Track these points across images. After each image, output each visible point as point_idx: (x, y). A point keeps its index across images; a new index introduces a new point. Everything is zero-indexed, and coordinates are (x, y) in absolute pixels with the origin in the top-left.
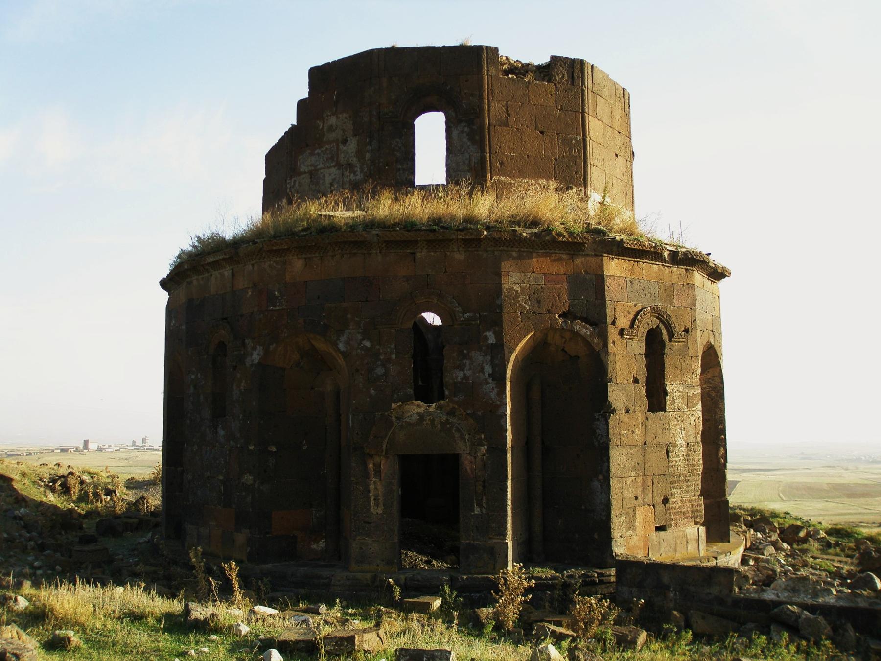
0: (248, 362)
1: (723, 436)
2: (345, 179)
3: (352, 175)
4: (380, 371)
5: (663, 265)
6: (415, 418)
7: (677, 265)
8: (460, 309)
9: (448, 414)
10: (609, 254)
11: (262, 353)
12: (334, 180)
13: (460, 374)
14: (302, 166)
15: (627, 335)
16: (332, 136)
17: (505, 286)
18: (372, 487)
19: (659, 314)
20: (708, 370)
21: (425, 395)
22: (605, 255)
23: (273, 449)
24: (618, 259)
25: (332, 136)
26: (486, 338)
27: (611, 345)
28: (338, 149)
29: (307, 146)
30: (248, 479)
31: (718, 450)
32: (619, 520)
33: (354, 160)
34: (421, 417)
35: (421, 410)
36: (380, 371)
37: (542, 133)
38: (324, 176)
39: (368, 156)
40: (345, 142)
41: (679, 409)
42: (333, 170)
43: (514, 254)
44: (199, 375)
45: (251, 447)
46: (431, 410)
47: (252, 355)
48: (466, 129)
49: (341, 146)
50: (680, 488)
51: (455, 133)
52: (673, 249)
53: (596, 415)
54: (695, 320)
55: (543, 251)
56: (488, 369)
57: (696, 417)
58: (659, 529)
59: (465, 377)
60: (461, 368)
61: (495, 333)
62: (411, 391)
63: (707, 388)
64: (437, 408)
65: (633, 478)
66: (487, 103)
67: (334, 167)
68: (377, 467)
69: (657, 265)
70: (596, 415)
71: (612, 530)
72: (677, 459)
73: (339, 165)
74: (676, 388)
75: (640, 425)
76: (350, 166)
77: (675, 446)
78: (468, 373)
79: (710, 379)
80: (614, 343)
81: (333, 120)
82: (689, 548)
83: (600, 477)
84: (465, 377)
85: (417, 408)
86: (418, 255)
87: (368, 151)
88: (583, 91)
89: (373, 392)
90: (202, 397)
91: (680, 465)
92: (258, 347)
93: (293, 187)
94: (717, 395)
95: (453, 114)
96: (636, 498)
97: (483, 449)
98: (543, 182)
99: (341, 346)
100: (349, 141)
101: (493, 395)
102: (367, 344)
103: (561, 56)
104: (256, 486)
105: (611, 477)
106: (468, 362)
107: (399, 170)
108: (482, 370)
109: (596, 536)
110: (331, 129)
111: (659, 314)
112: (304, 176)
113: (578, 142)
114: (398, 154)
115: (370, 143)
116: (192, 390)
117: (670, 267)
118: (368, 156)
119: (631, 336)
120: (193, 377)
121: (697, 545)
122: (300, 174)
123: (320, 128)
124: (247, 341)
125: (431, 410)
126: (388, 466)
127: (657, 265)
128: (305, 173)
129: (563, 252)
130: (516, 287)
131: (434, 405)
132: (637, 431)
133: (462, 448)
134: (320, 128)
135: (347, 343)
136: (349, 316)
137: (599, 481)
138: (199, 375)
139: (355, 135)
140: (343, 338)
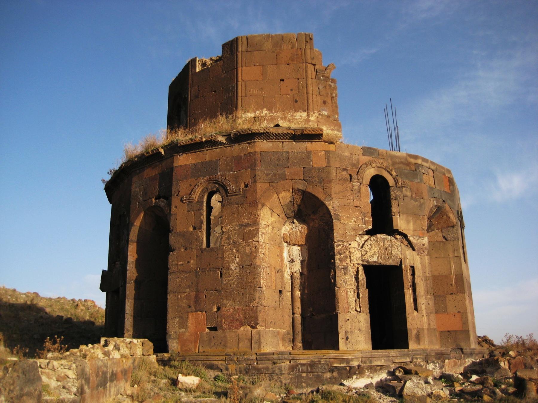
1: (332, 261)
5: (225, 147)
7: (238, 142)
10: (177, 153)
15: (186, 200)
17: (133, 190)
19: (215, 180)
20: (319, 210)
22: (174, 155)
24: (186, 154)
27: (173, 208)
31: (330, 272)
32: (174, 321)
41: (234, 243)
43: (138, 171)
50: (233, 300)
52: (302, 129)
54: (255, 176)
55: (149, 164)
57: (252, 247)
63: (322, 224)
65: (187, 293)
66: (190, 90)
69: (219, 148)
71: (167, 327)
72: (230, 278)
74: (231, 228)
75: (195, 257)
77: (228, 268)
79: (322, 217)
80: (176, 207)
82: (240, 345)
88: (237, 55)
91: (233, 283)
94: (328, 228)
96: (190, 307)
103: (226, 42)
105: (168, 292)
111: (215, 180)
113: (233, 87)
117: (233, 146)
119: (189, 200)
121: (249, 344)
127: (219, 148)
129: (157, 161)
132: (192, 261)
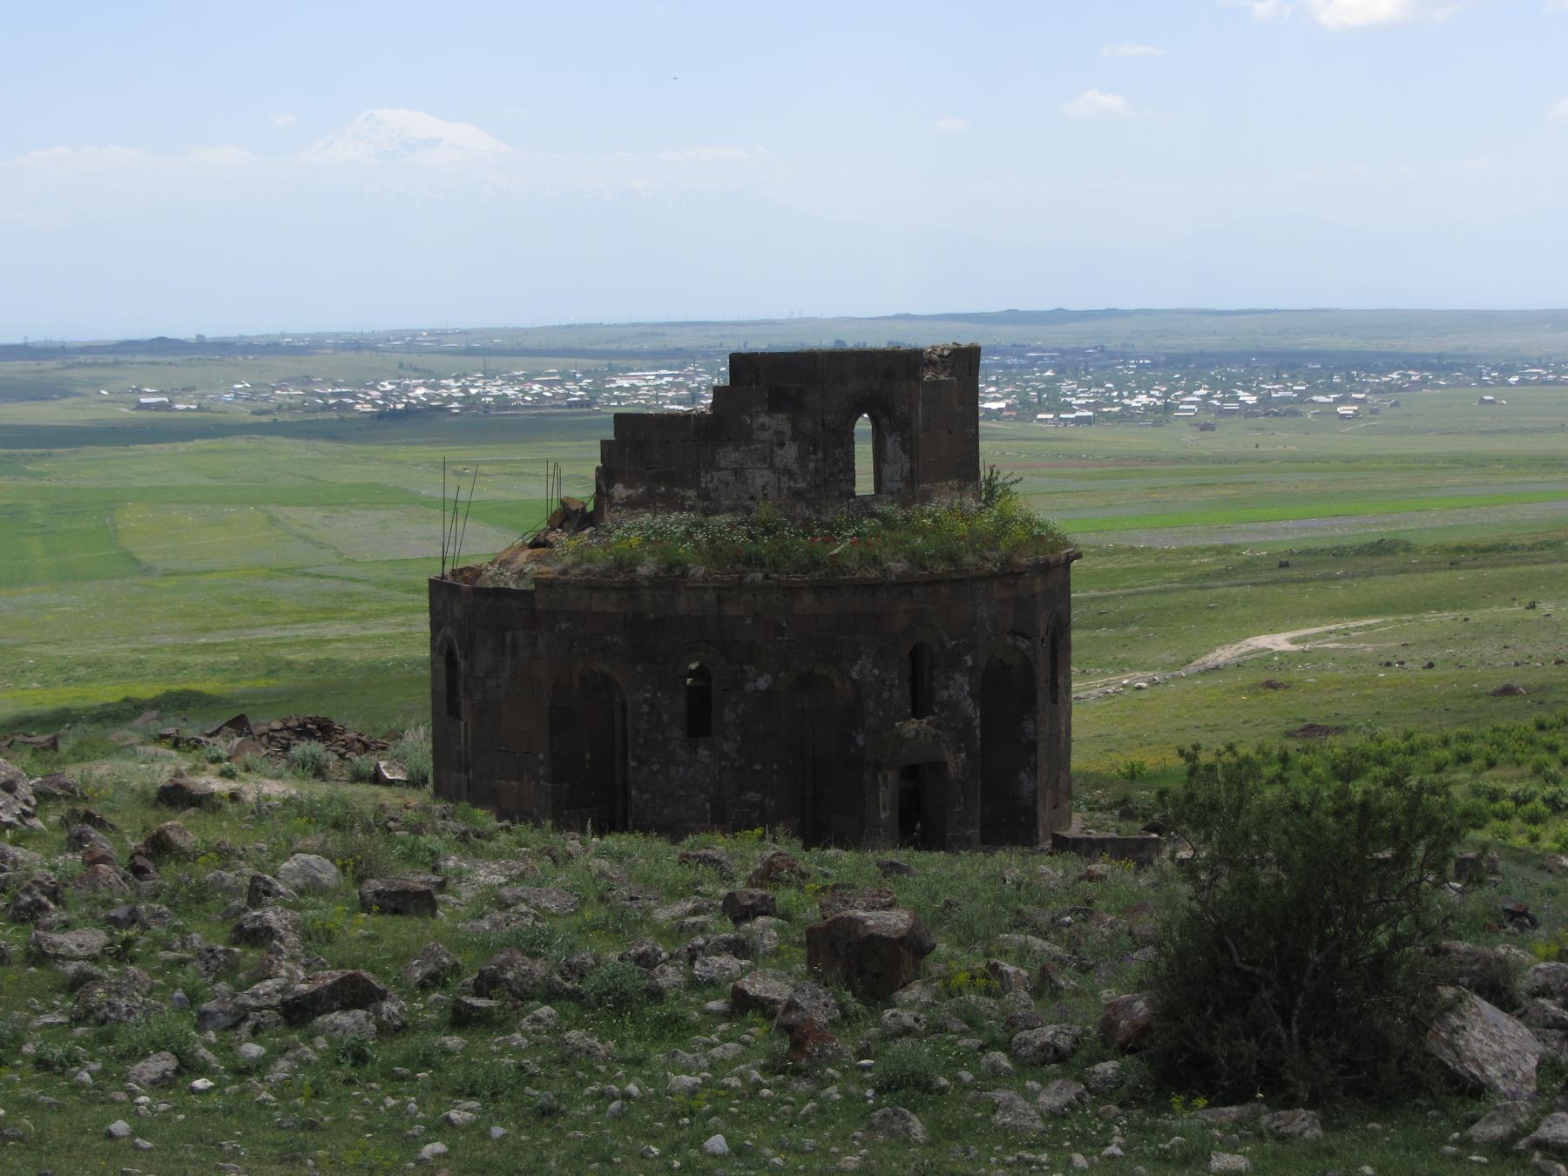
0: (749, 687)
2: (782, 485)
3: (792, 482)
4: (886, 695)
6: (913, 733)
8: (947, 638)
9: (935, 727)
11: (771, 680)
12: (767, 483)
13: (946, 694)
14: (722, 461)
16: (765, 435)
18: (881, 795)
21: (917, 713)
23: (775, 767)
25: (765, 435)
26: (966, 662)
28: (772, 450)
29: (729, 439)
30: (754, 796)
33: (795, 468)
34: (918, 733)
35: (915, 726)
36: (886, 695)
37: (950, 432)
38: (754, 477)
39: (812, 465)
40: (781, 445)
42: (767, 473)
44: (659, 694)
45: (758, 767)
46: (923, 725)
47: (755, 681)
48: (899, 438)
49: (776, 449)
51: (889, 443)
53: (1025, 716)
56: (967, 688)
58: (1055, 807)
59: (950, 696)
60: (947, 688)
61: (972, 656)
62: (909, 711)
64: (929, 723)
67: (768, 469)
68: (885, 778)
70: (1025, 716)
73: (772, 467)
76: (789, 473)
78: (952, 692)
81: (764, 419)
83: (1028, 769)
84: (950, 696)
85: (913, 726)
86: (915, 591)
87: (812, 460)
89: (881, 714)
90: (666, 717)
92: (765, 674)
93: (711, 482)
95: (888, 422)
97: (963, 755)
98: (950, 483)
99: (854, 675)
100: (787, 446)
101: (970, 709)
102: (876, 672)
104: (767, 802)
106: (951, 683)
107: (841, 481)
108: (962, 690)
109: (1023, 820)
110: (762, 427)
112: (726, 472)
114: (841, 464)
115: (815, 452)
116: (645, 708)
118: (812, 465)
120: (648, 695)
122: (719, 469)
123: (749, 422)
124: (746, 667)
125: (923, 725)
126: (892, 776)
128: (727, 469)
130: (985, 615)
131: (925, 721)
133: (948, 756)
134: (749, 422)
135: (860, 672)
136: (862, 648)
137: (1026, 772)
138: (659, 694)
139: (794, 439)
140: (857, 668)
